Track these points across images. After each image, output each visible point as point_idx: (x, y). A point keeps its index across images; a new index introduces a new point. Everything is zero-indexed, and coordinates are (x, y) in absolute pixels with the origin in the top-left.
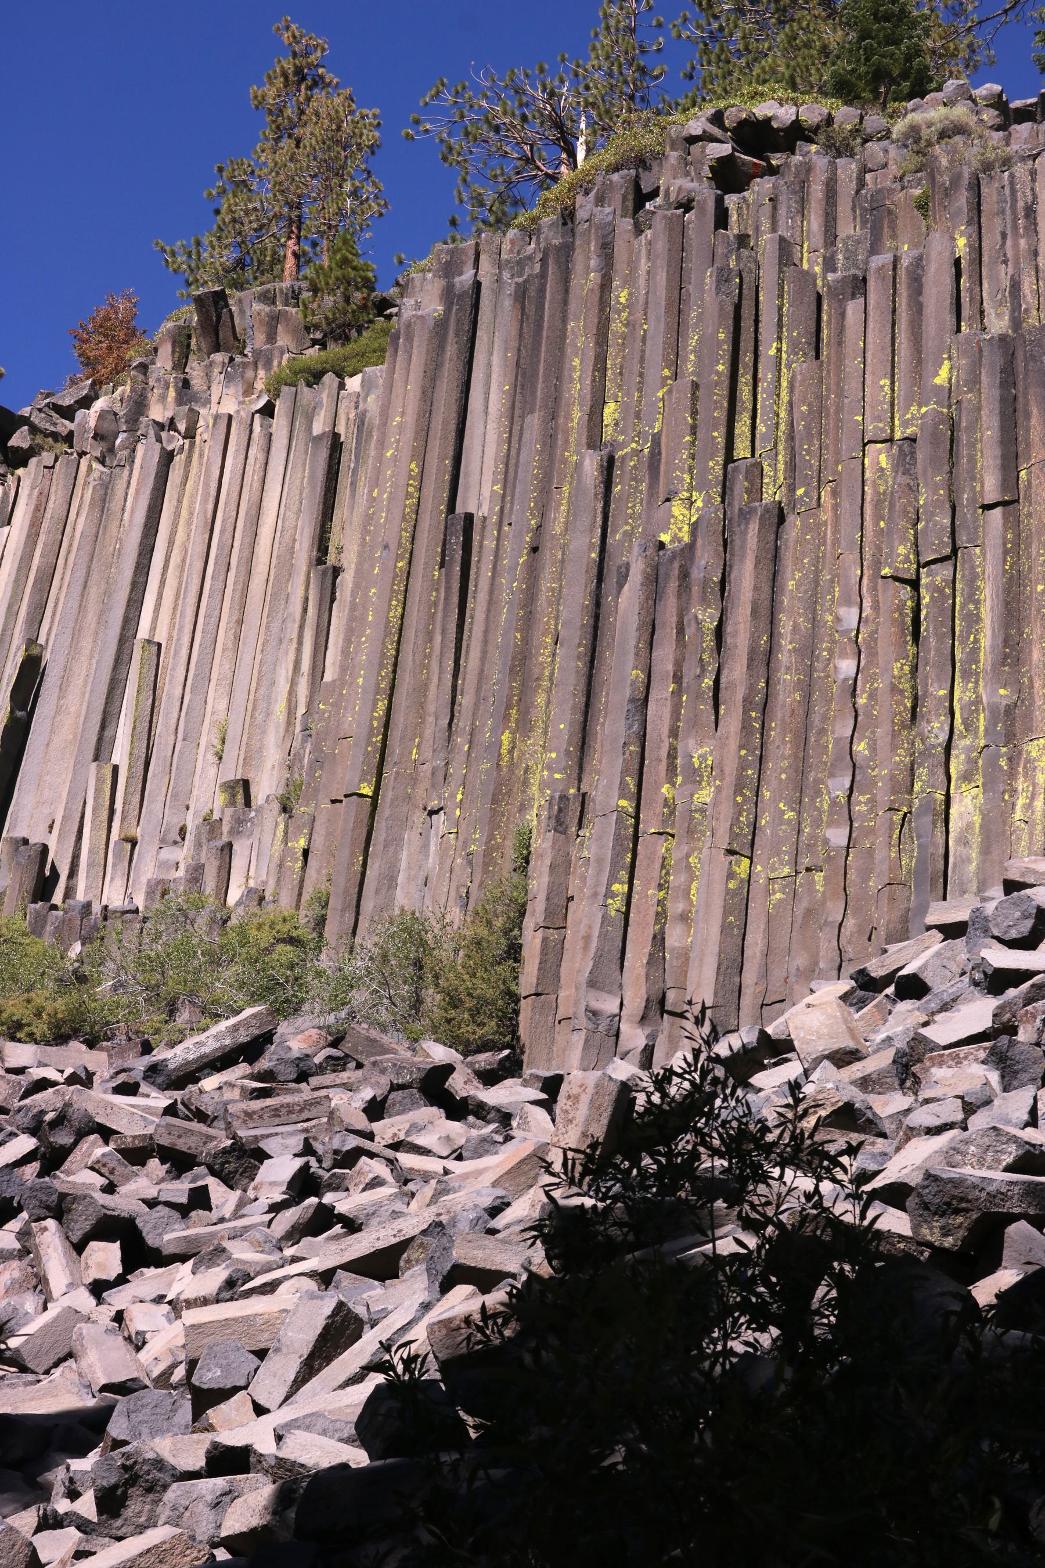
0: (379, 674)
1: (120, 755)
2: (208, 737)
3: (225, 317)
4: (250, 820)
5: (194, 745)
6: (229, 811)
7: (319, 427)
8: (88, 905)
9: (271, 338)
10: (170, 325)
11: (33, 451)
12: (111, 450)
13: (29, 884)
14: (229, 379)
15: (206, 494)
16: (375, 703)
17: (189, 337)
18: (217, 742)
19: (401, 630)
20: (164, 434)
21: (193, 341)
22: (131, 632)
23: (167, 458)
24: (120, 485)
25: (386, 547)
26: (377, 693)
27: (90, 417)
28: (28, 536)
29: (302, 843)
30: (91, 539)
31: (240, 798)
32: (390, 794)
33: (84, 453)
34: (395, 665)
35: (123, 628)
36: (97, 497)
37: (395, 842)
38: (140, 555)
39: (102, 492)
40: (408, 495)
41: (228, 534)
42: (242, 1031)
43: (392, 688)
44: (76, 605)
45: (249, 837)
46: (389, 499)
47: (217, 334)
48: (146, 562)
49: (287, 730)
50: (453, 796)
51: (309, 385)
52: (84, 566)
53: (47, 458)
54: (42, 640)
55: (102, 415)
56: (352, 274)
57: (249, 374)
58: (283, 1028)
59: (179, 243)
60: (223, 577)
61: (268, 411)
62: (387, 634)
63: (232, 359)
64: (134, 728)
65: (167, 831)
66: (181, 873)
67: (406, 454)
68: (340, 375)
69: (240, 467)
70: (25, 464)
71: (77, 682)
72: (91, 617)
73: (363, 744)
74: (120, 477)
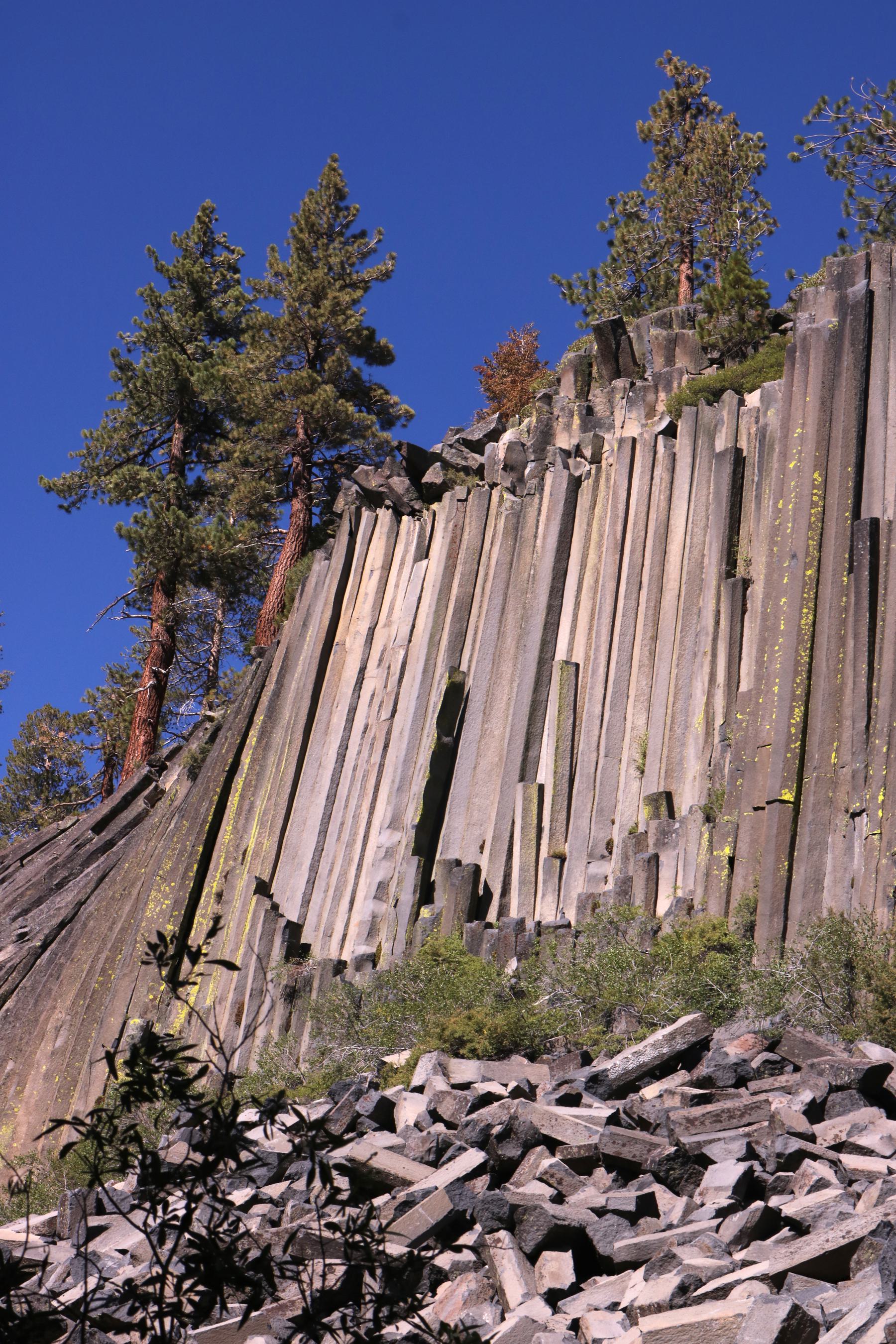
0: (794, 682)
1: (545, 775)
2: (629, 752)
3: (624, 344)
4: (675, 831)
6: (654, 824)
7: (721, 443)
8: (521, 923)
9: (670, 360)
10: (571, 355)
11: (446, 486)
12: (521, 480)
13: (464, 903)
14: (631, 403)
15: (615, 516)
16: (792, 709)
17: (591, 365)
18: (638, 757)
19: (813, 636)
20: (571, 461)
21: (595, 370)
22: (549, 655)
23: (576, 483)
24: (532, 513)
25: (794, 556)
26: (793, 700)
27: (499, 449)
28: (446, 568)
29: (727, 851)
30: (505, 567)
31: (664, 810)
32: (811, 799)
33: (496, 485)
34: (810, 671)
35: (542, 651)
36: (510, 527)
37: (819, 846)
38: (554, 579)
39: (514, 521)
40: (813, 504)
41: (638, 554)
42: (679, 1039)
43: (808, 694)
44: (495, 631)
45: (675, 847)
46: (795, 509)
47: (617, 361)
48: (560, 585)
49: (706, 742)
50: (874, 797)
51: (710, 404)
52: (501, 593)
53: (460, 491)
54: (464, 668)
55: (510, 447)
56: (746, 292)
57: (651, 397)
58: (719, 1034)
60: (635, 596)
61: (670, 432)
62: (800, 641)
63: (632, 384)
64: (557, 748)
65: (595, 846)
66: (610, 886)
67: (809, 463)
68: (739, 391)
69: (646, 488)
70: (439, 499)
71: (500, 705)
72: (510, 642)
73: (782, 751)
74: (531, 505)
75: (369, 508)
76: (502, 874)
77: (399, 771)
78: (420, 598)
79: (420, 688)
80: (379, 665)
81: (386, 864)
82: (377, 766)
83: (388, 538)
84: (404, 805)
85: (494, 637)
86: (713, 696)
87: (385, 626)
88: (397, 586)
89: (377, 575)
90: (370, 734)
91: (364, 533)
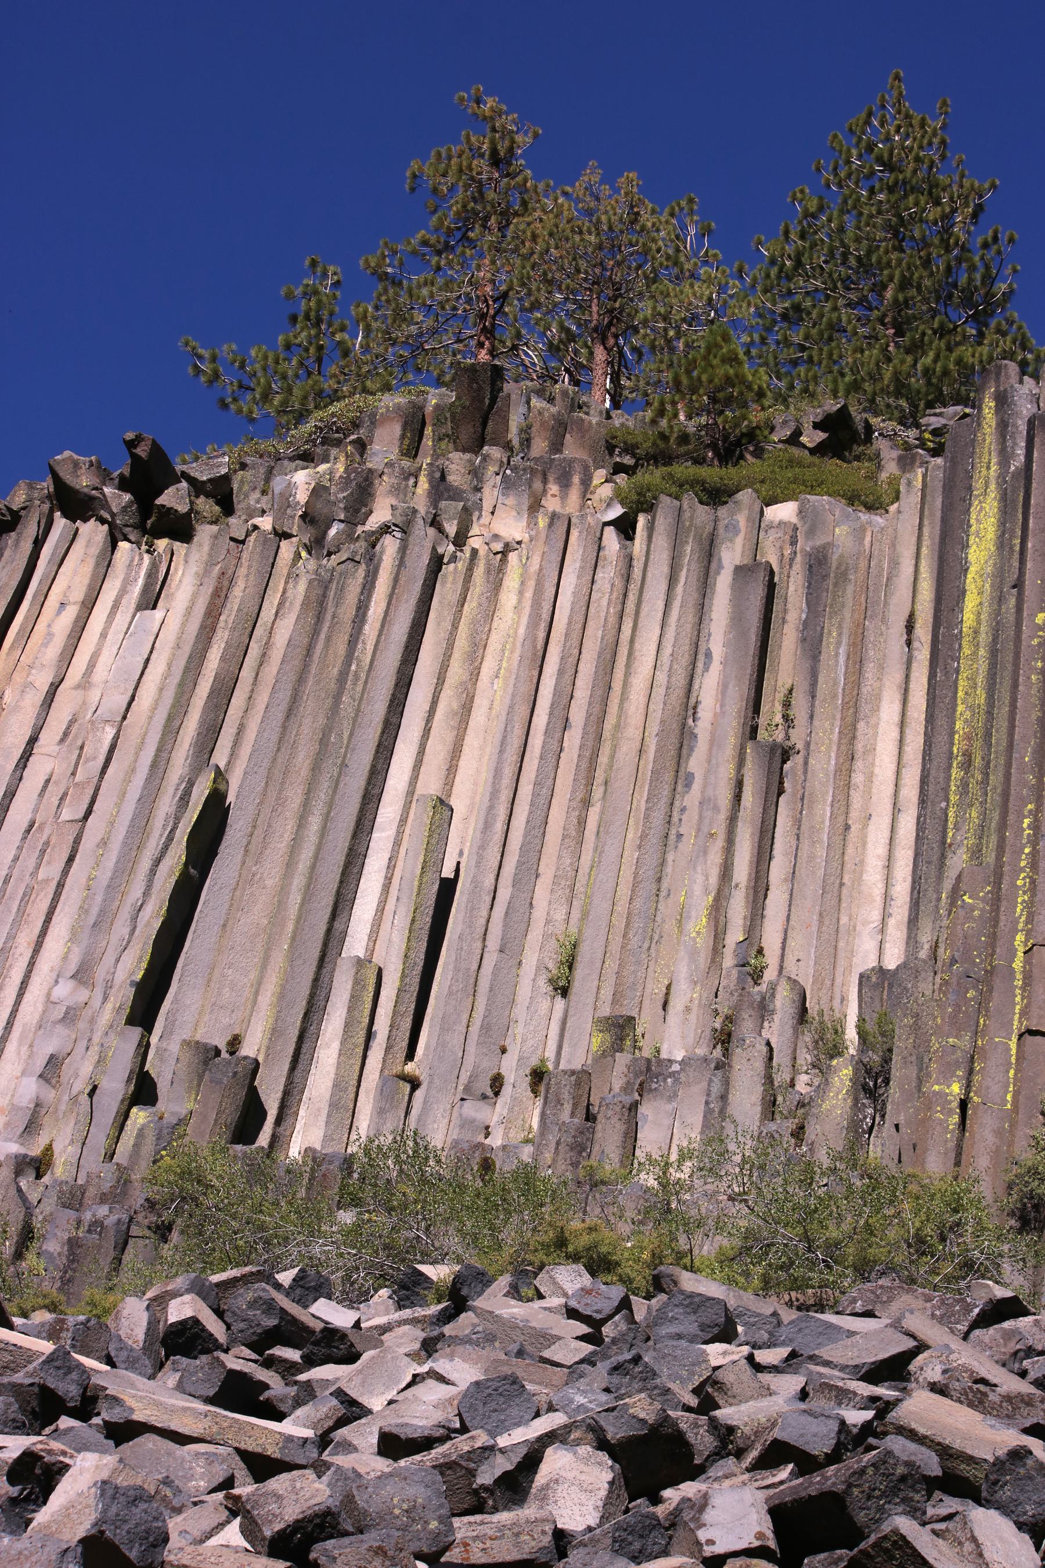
4: (672, 1075)
5: (515, 962)
9: (557, 446)
13: (231, 1115)
22: (377, 791)
23: (437, 563)
30: (300, 652)
35: (369, 781)
36: (313, 598)
38: (396, 685)
39: (320, 592)
44: (275, 738)
45: (670, 1099)
47: (484, 424)
49: (713, 961)
52: (290, 686)
59: (225, 347)
60: (558, 735)
64: (413, 921)
74: (353, 574)
75: (66, 515)
76: (281, 1088)
77: (99, 899)
78: (148, 660)
79: (144, 788)
80: (62, 741)
81: (61, 1030)
82: (53, 885)
83: (97, 564)
84: (100, 950)
85: (273, 746)
86: (728, 898)
87: (78, 687)
88: (104, 635)
89: (71, 613)
90: (38, 839)
91: (56, 547)
